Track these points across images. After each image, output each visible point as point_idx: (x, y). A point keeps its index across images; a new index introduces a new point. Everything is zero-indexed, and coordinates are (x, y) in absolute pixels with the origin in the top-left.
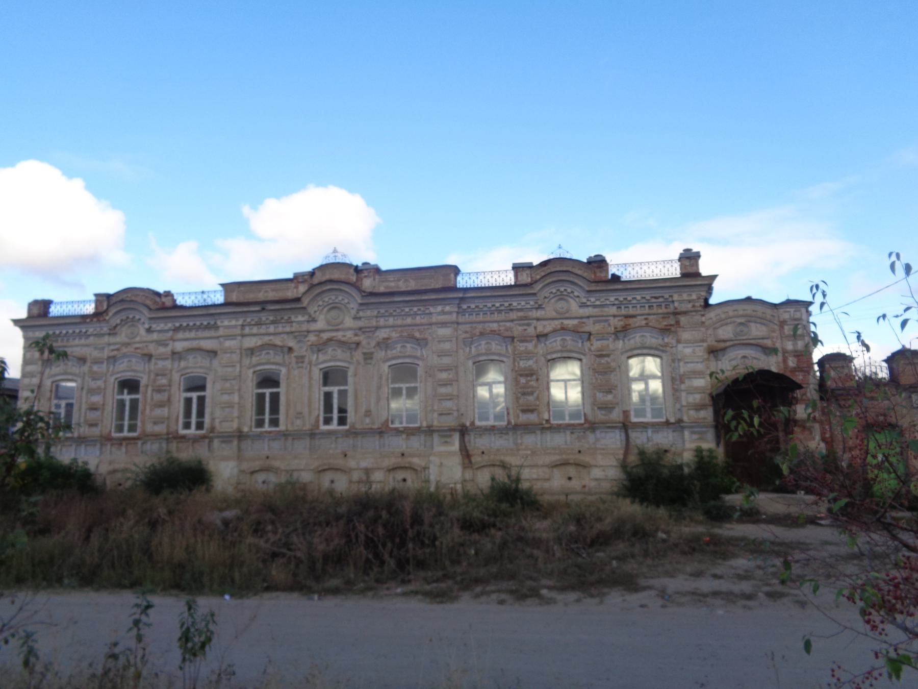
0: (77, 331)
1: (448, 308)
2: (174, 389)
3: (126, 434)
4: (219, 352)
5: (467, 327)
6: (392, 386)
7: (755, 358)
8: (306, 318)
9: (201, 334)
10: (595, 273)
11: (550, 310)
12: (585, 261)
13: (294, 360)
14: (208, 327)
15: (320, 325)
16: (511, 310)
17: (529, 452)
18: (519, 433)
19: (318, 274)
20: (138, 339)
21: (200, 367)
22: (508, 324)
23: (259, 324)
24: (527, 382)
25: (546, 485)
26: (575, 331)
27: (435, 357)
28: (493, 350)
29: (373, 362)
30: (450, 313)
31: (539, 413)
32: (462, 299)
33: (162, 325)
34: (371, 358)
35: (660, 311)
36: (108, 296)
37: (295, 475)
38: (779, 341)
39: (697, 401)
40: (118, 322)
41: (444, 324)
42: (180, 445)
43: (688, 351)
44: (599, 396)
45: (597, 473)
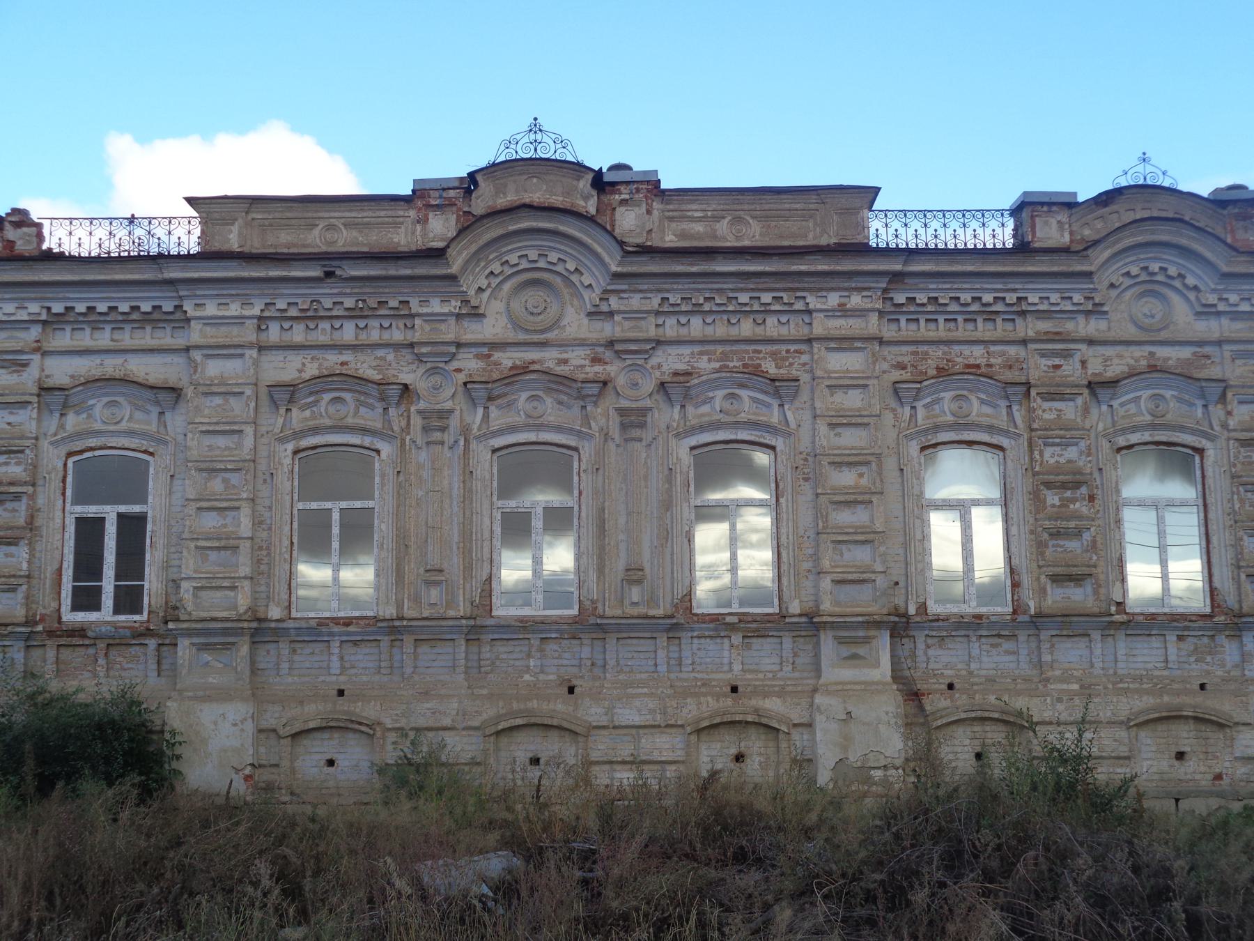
1: (856, 300)
2: (47, 495)
4: (190, 392)
5: (903, 354)
6: (301, 505)
8: (454, 305)
9: (127, 338)
11: (1119, 322)
12: (1205, 194)
13: (417, 422)
14: (153, 319)
15: (493, 326)
17: (1076, 687)
18: (1045, 635)
21: (131, 433)
22: (1012, 350)
23: (309, 317)
24: (1065, 503)
26: (1185, 376)
27: (822, 428)
28: (973, 417)
29: (647, 435)
30: (861, 313)
33: (9, 308)
34: (642, 425)
41: (844, 342)
42: (66, 654)
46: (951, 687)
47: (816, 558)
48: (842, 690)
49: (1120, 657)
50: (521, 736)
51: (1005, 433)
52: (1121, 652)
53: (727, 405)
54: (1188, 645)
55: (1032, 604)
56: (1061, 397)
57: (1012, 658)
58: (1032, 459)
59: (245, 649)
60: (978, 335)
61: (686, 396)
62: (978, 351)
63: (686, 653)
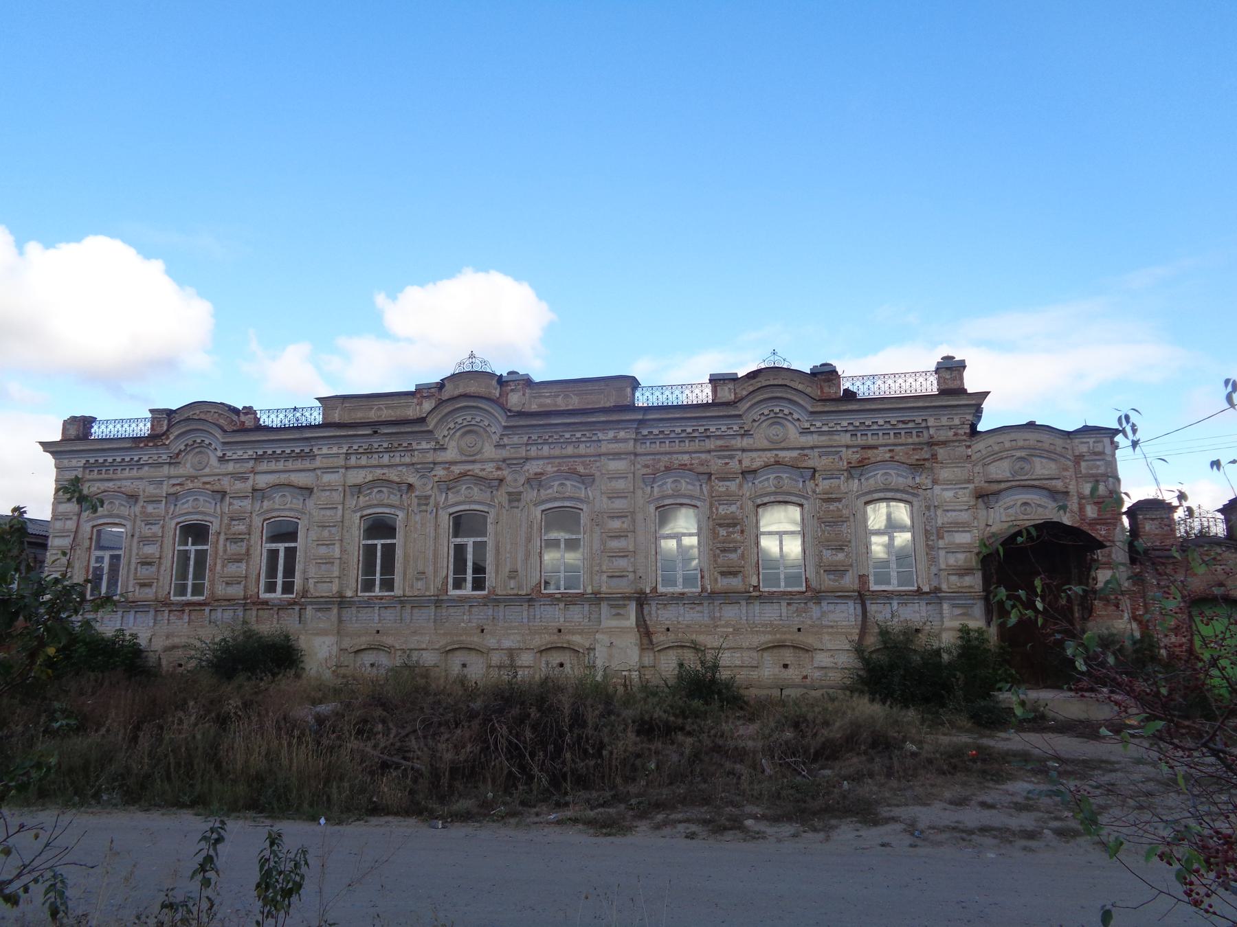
0: (127, 459)
1: (622, 434)
2: (255, 537)
3: (189, 597)
5: (648, 460)
7: (1039, 505)
9: (290, 465)
10: (822, 388)
13: (415, 501)
14: (301, 456)
15: (451, 454)
16: (708, 437)
18: (717, 603)
19: (448, 386)
20: (207, 470)
21: (291, 510)
22: (703, 456)
23: (369, 452)
24: (729, 534)
25: (754, 674)
27: (605, 500)
28: (683, 491)
29: (521, 505)
30: (625, 440)
31: (744, 577)
32: (641, 422)
33: (240, 453)
34: (519, 500)
35: (910, 441)
36: (169, 413)
37: (415, 655)
38: (1074, 482)
39: (960, 563)
40: (182, 447)
41: (616, 456)
42: (261, 612)
43: (948, 495)
44: (827, 554)
45: (822, 659)
47: (600, 565)
48: (610, 631)
50: (458, 653)
51: (698, 499)
53: (560, 489)
54: (794, 607)
56: (728, 479)
58: (712, 512)
59: (335, 611)
60: (686, 449)
61: (540, 485)
62: (686, 457)
63: (538, 613)
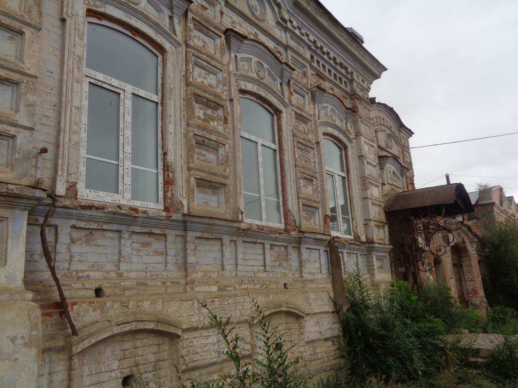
17: (215, 289)
18: (191, 235)
24: (208, 119)
46: (98, 292)
49: (240, 262)
52: (240, 256)
55: (185, 203)
57: (160, 259)
